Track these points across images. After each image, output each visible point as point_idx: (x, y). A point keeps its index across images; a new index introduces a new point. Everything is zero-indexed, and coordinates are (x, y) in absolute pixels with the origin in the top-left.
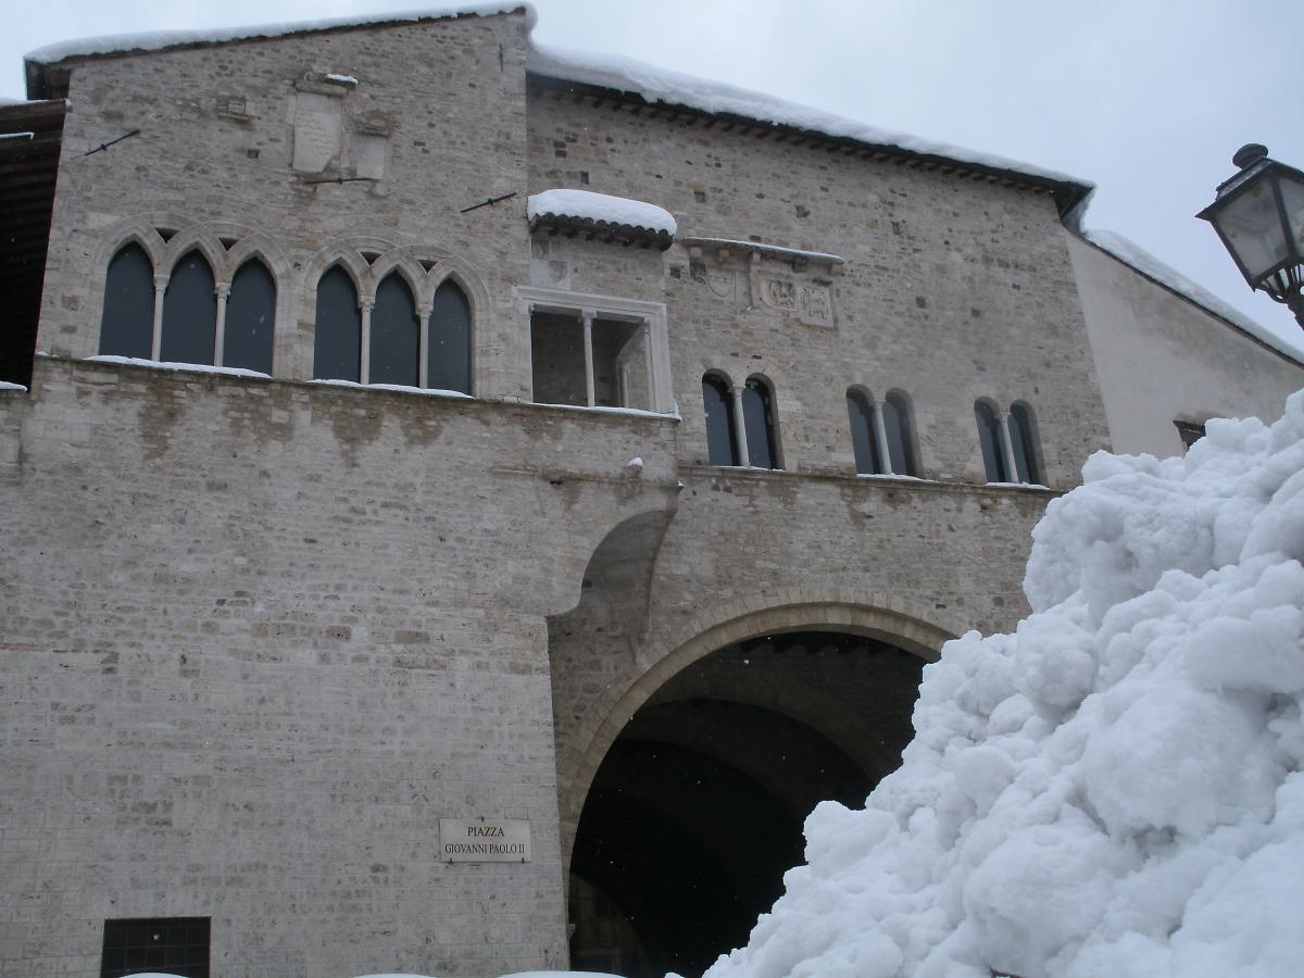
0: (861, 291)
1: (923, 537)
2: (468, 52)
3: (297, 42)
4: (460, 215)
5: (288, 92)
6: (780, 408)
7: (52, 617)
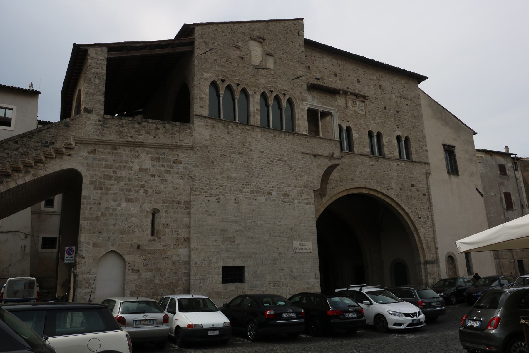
0: (372, 104)
1: (384, 172)
2: (291, 31)
3: (250, 24)
4: (291, 81)
5: (249, 40)
6: (353, 136)
7: (204, 187)
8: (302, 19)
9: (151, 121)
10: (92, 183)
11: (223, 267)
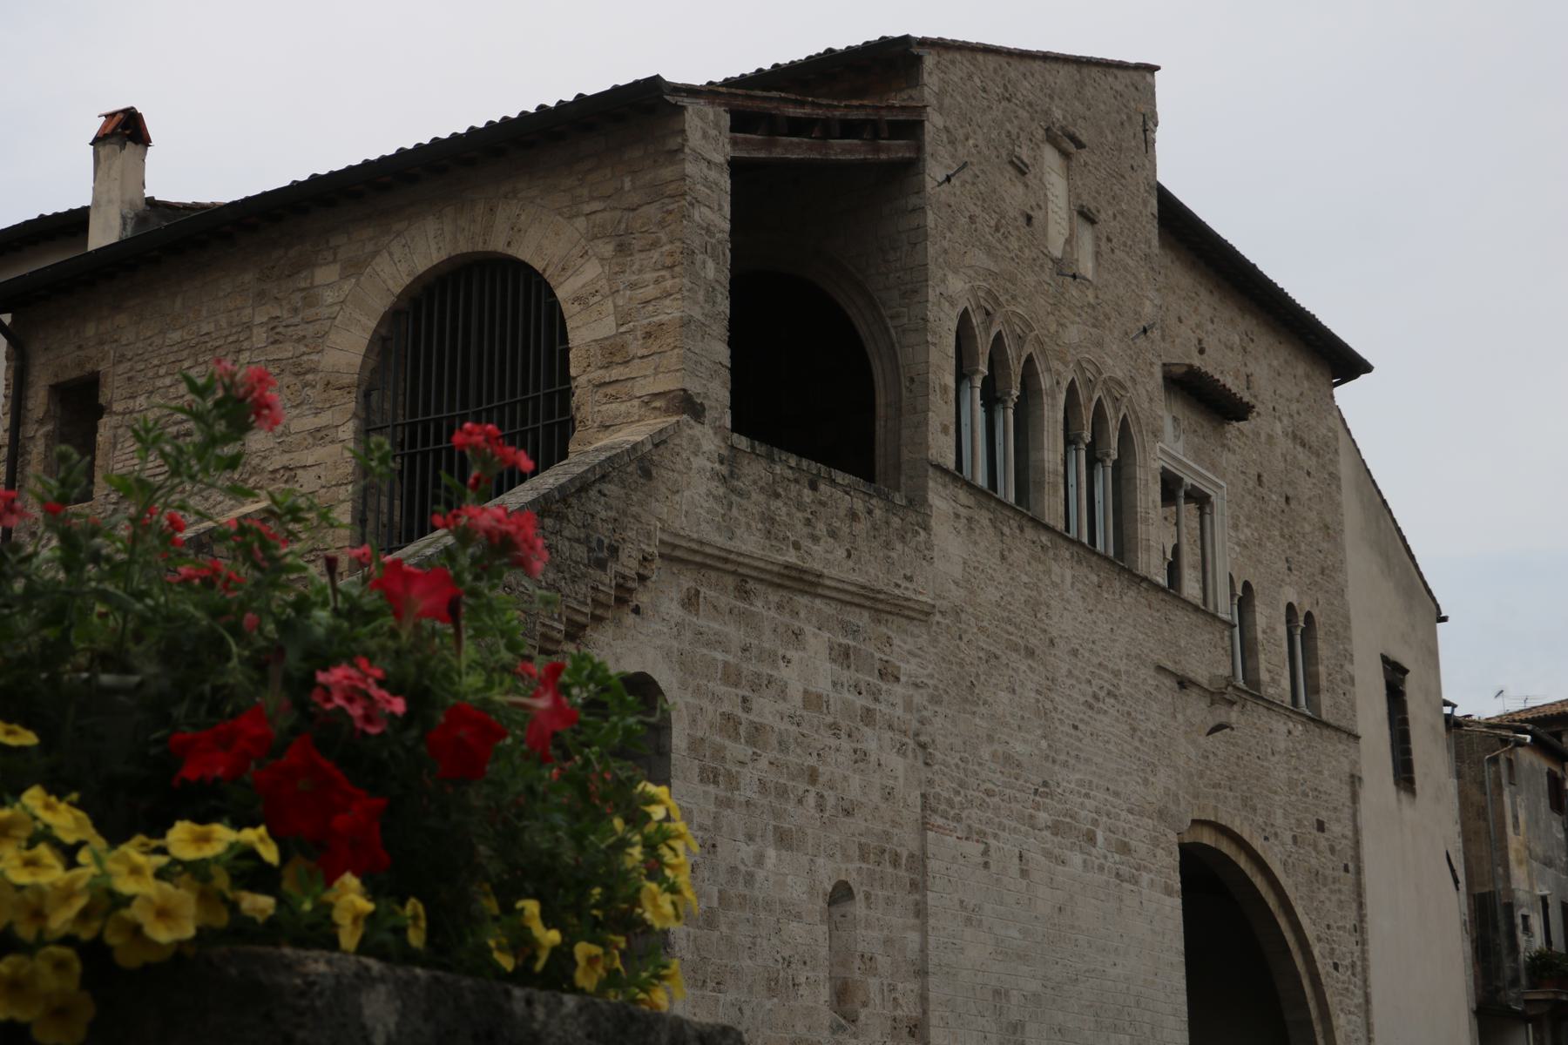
5: (1043, 142)
9: (841, 478)
10: (695, 745)
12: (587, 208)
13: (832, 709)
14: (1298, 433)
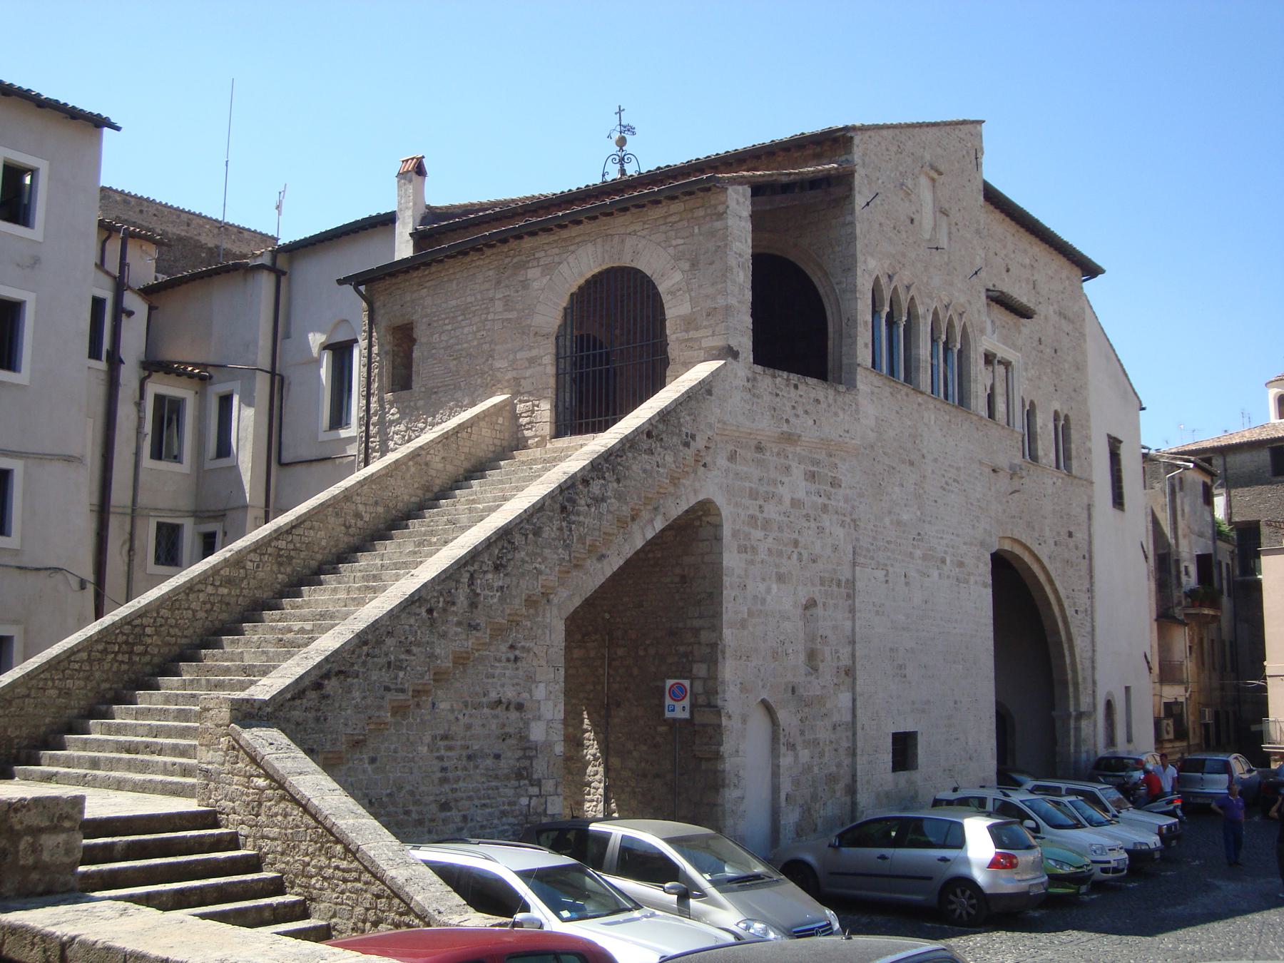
8: (980, 122)
9: (810, 380)
10: (735, 534)
11: (894, 734)
12: (674, 243)
13: (806, 506)
14: (1062, 311)
